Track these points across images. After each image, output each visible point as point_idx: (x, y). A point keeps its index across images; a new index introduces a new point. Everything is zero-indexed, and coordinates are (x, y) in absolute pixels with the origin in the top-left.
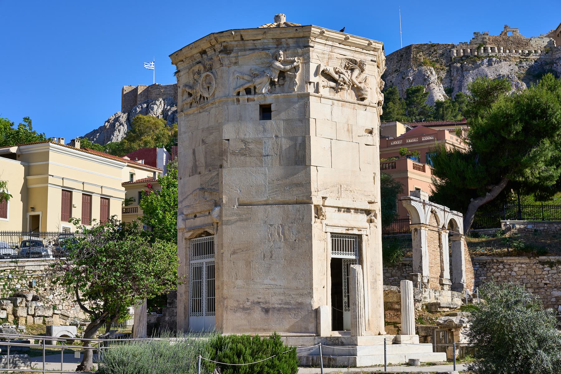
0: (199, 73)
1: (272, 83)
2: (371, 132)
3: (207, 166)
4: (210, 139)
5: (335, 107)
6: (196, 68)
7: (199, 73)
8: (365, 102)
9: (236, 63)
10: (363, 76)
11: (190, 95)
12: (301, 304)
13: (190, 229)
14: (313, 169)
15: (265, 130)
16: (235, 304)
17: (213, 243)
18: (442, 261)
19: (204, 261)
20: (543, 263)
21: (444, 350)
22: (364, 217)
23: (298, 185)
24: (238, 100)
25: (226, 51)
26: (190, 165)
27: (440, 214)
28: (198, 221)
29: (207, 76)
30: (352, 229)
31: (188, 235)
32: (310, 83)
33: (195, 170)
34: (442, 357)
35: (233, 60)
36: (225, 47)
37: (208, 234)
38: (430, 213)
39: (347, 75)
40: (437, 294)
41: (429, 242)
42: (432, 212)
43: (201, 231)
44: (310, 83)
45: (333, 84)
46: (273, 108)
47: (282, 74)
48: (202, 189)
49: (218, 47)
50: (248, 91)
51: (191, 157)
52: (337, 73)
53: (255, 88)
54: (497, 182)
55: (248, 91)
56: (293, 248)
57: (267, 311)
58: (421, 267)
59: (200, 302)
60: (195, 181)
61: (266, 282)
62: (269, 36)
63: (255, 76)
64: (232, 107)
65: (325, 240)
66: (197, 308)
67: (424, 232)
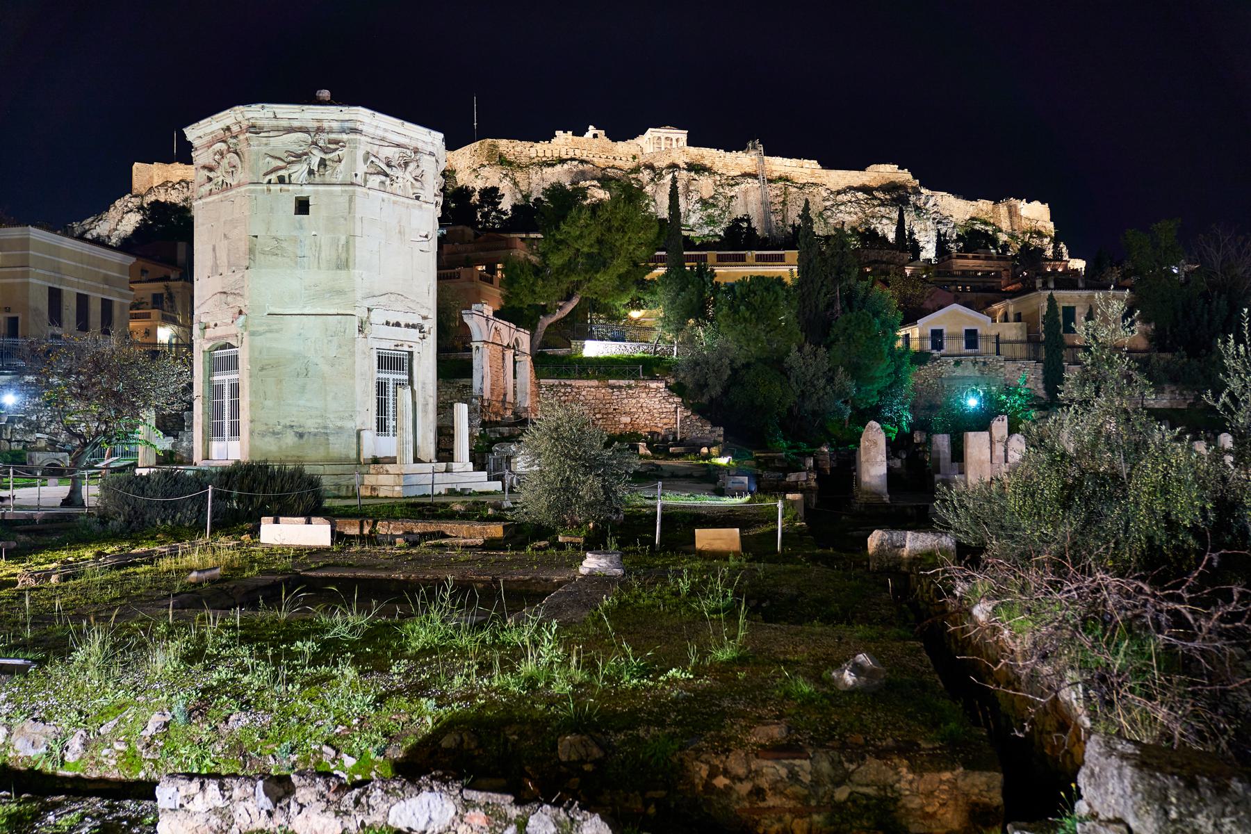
1: (311, 172)
3: (229, 266)
13: (210, 339)
15: (301, 227)
16: (264, 428)
19: (226, 377)
20: (613, 387)
21: (500, 478)
23: (340, 292)
26: (210, 263)
28: (219, 332)
31: (207, 347)
33: (215, 271)
34: (497, 486)
36: (253, 126)
37: (232, 347)
43: (222, 342)
45: (383, 178)
49: (245, 124)
51: (211, 252)
52: (388, 165)
53: (290, 176)
54: (568, 298)
57: (301, 436)
58: (481, 389)
60: (216, 284)
61: (301, 402)
66: (214, 431)
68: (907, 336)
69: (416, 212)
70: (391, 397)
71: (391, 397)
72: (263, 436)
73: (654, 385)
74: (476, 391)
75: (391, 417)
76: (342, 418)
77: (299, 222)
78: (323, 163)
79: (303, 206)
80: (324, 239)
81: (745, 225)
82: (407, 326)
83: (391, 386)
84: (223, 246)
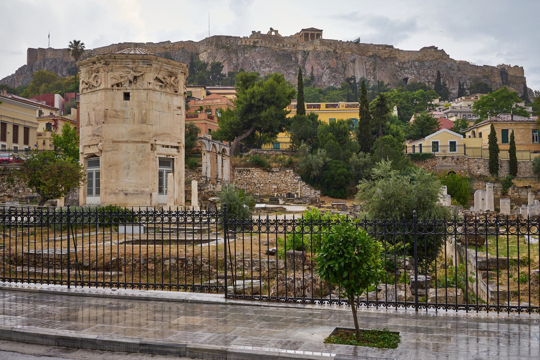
1: (130, 82)
2: (180, 108)
4: (98, 108)
7: (92, 74)
8: (178, 93)
9: (112, 71)
10: (177, 80)
11: (87, 84)
12: (143, 191)
15: (126, 106)
16: (111, 191)
17: (99, 161)
18: (217, 169)
19: (94, 169)
22: (175, 150)
23: (143, 134)
24: (113, 89)
26: (87, 120)
27: (217, 146)
29: (96, 76)
30: (169, 156)
31: (86, 156)
32: (150, 83)
33: (89, 124)
35: (110, 69)
38: (212, 146)
39: (168, 80)
40: (214, 186)
41: (211, 160)
42: (213, 145)
44: (150, 83)
45: (161, 84)
46: (130, 94)
47: (135, 78)
50: (118, 85)
51: (87, 116)
54: (249, 128)
55: (118, 85)
56: (140, 165)
57: (126, 194)
59: (92, 190)
61: (126, 180)
63: (121, 77)
64: (110, 93)
66: (90, 193)
68: (421, 145)
69: (175, 98)
70: (165, 178)
71: (165, 178)
72: (110, 194)
73: (288, 171)
74: (203, 173)
75: (165, 186)
76: (144, 187)
77: (126, 104)
78: (135, 78)
79: (127, 96)
80: (136, 111)
81: (352, 82)
82: (172, 147)
83: (165, 173)
84: (92, 114)
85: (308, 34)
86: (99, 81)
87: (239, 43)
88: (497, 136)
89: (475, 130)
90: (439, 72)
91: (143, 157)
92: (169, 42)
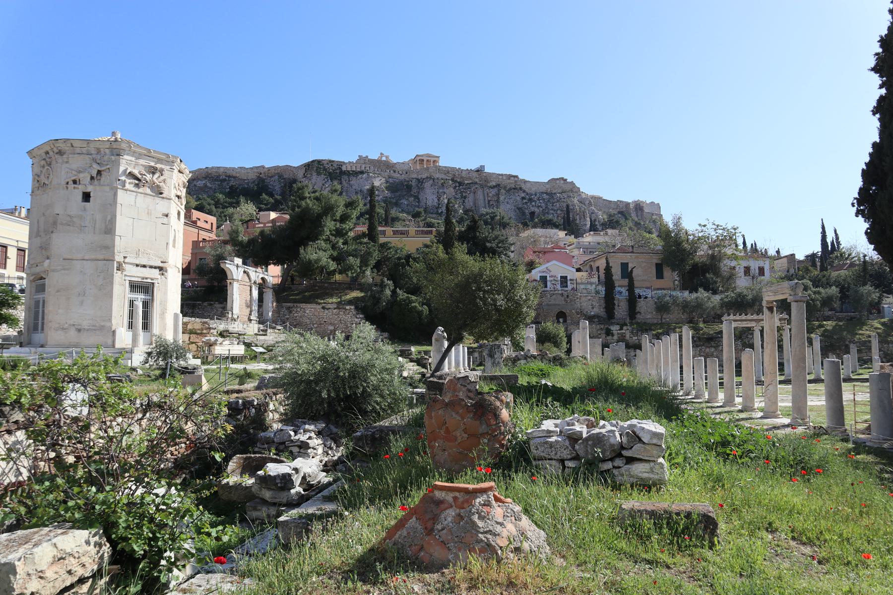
0: (43, 167)
1: (92, 178)
2: (167, 216)
5: (138, 198)
6: (43, 162)
7: (43, 167)
9: (67, 162)
10: (162, 178)
14: (117, 239)
15: (85, 210)
17: (44, 285)
25: (60, 153)
26: (35, 230)
35: (66, 160)
39: (149, 177)
40: (245, 326)
42: (245, 272)
46: (92, 195)
48: (41, 248)
49: (56, 150)
50: (75, 182)
55: (75, 182)
56: (100, 290)
57: (79, 330)
62: (92, 145)
63: (80, 172)
65: (124, 285)
67: (236, 285)
73: (348, 307)
76: (104, 321)
78: (99, 173)
79: (86, 197)
82: (151, 267)
85: (423, 160)
86: (51, 176)
87: (344, 168)
88: (613, 270)
89: (592, 263)
90: (568, 206)
91: (104, 279)
92: (263, 167)
